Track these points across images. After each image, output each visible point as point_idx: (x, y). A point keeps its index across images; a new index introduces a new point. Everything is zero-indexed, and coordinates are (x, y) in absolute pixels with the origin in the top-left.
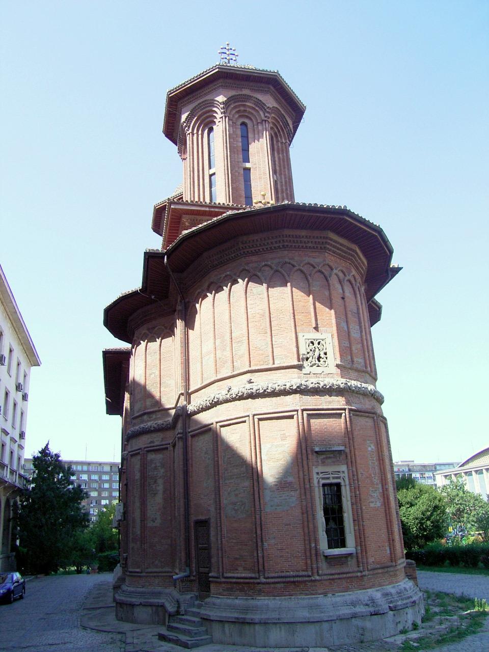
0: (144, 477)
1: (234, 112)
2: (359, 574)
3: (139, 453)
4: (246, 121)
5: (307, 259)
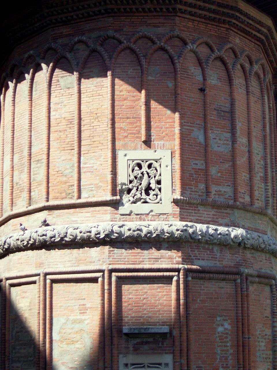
5: (145, 30)
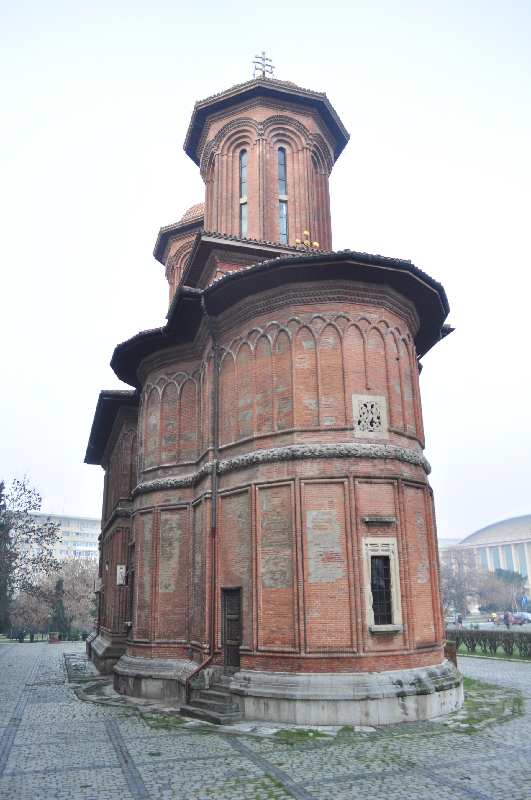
0: (156, 538)
1: (273, 134)
2: (405, 652)
3: (151, 512)
4: (285, 146)
5: (363, 314)
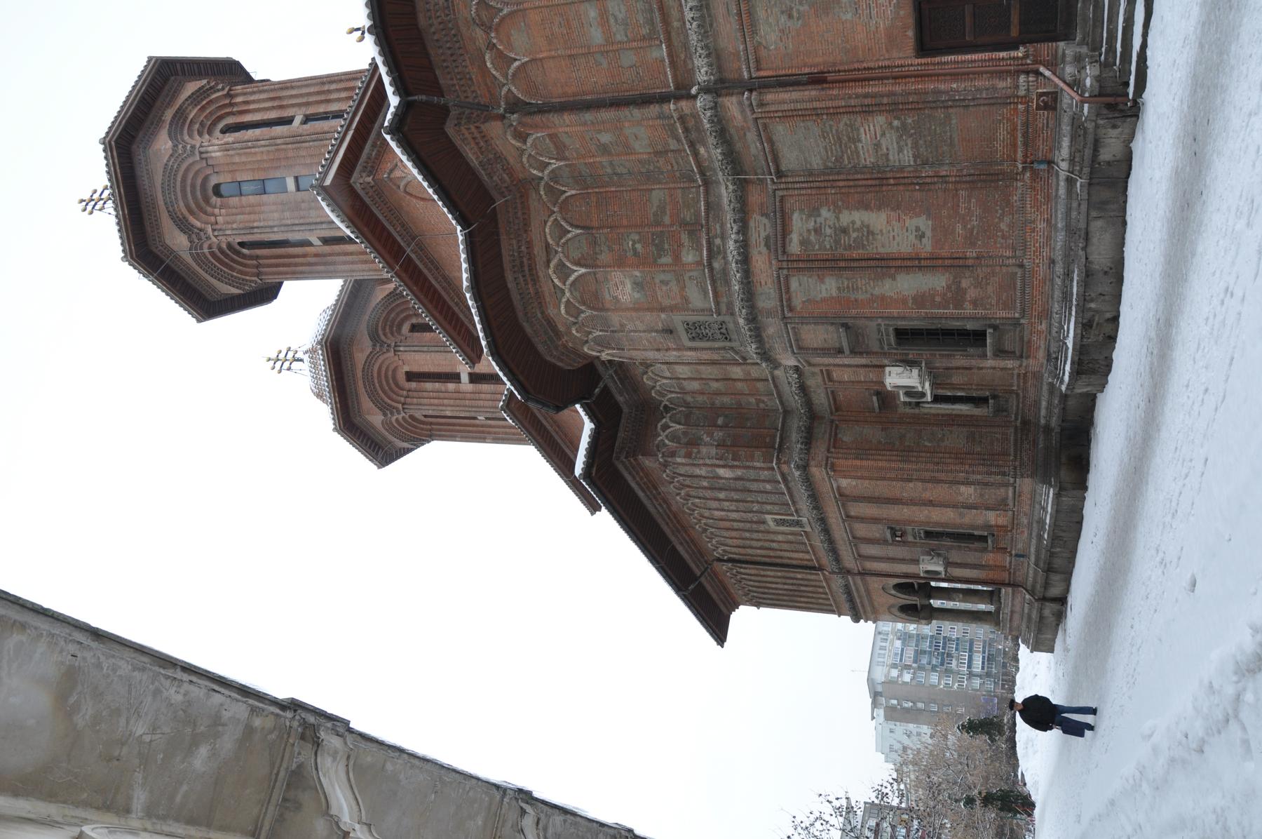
4: (221, 125)
